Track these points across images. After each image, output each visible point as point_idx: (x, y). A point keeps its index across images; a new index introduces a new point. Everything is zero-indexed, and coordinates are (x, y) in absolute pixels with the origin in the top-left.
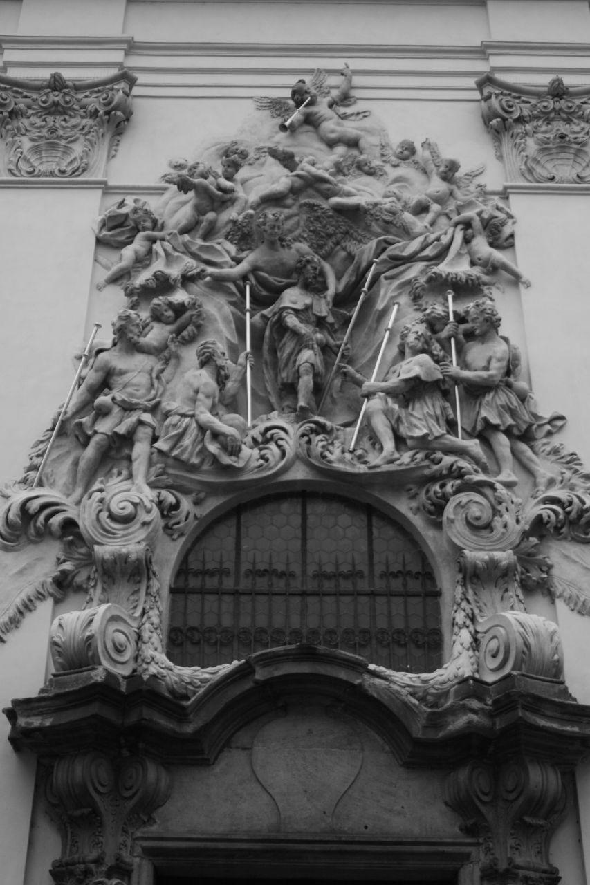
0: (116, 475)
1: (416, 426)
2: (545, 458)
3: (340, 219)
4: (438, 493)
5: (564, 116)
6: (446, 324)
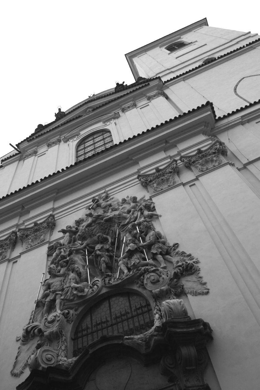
2: (175, 257)
5: (162, 175)
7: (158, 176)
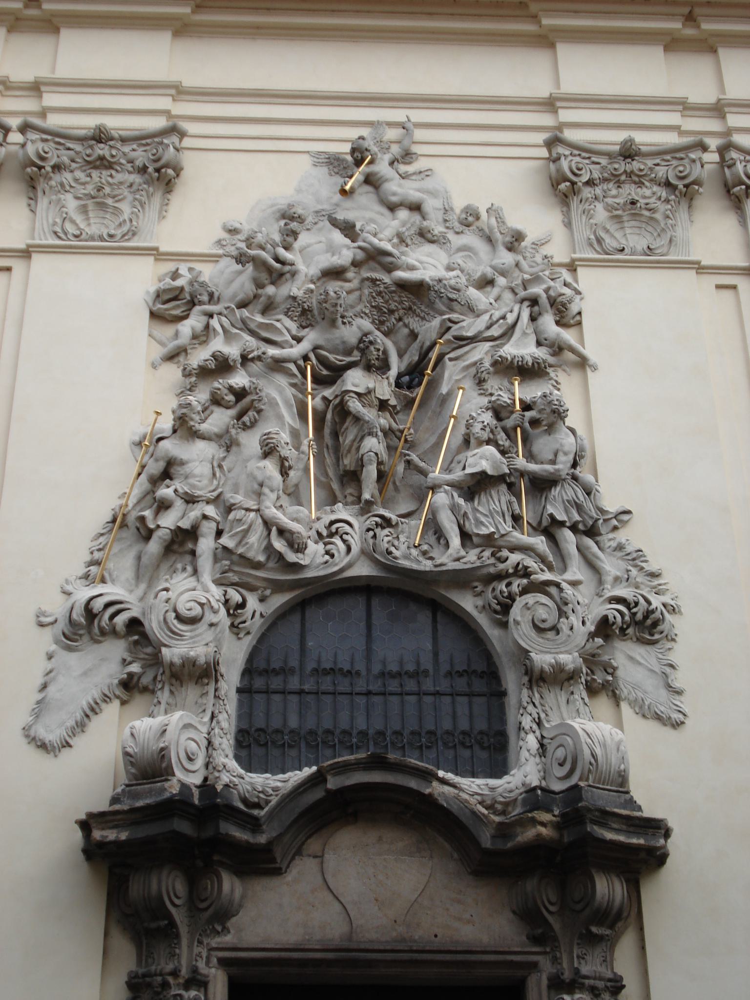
0: (180, 570)
1: (482, 523)
2: (610, 555)
3: (403, 295)
4: (504, 592)
5: (637, 179)
6: (512, 412)
7: (620, 175)
